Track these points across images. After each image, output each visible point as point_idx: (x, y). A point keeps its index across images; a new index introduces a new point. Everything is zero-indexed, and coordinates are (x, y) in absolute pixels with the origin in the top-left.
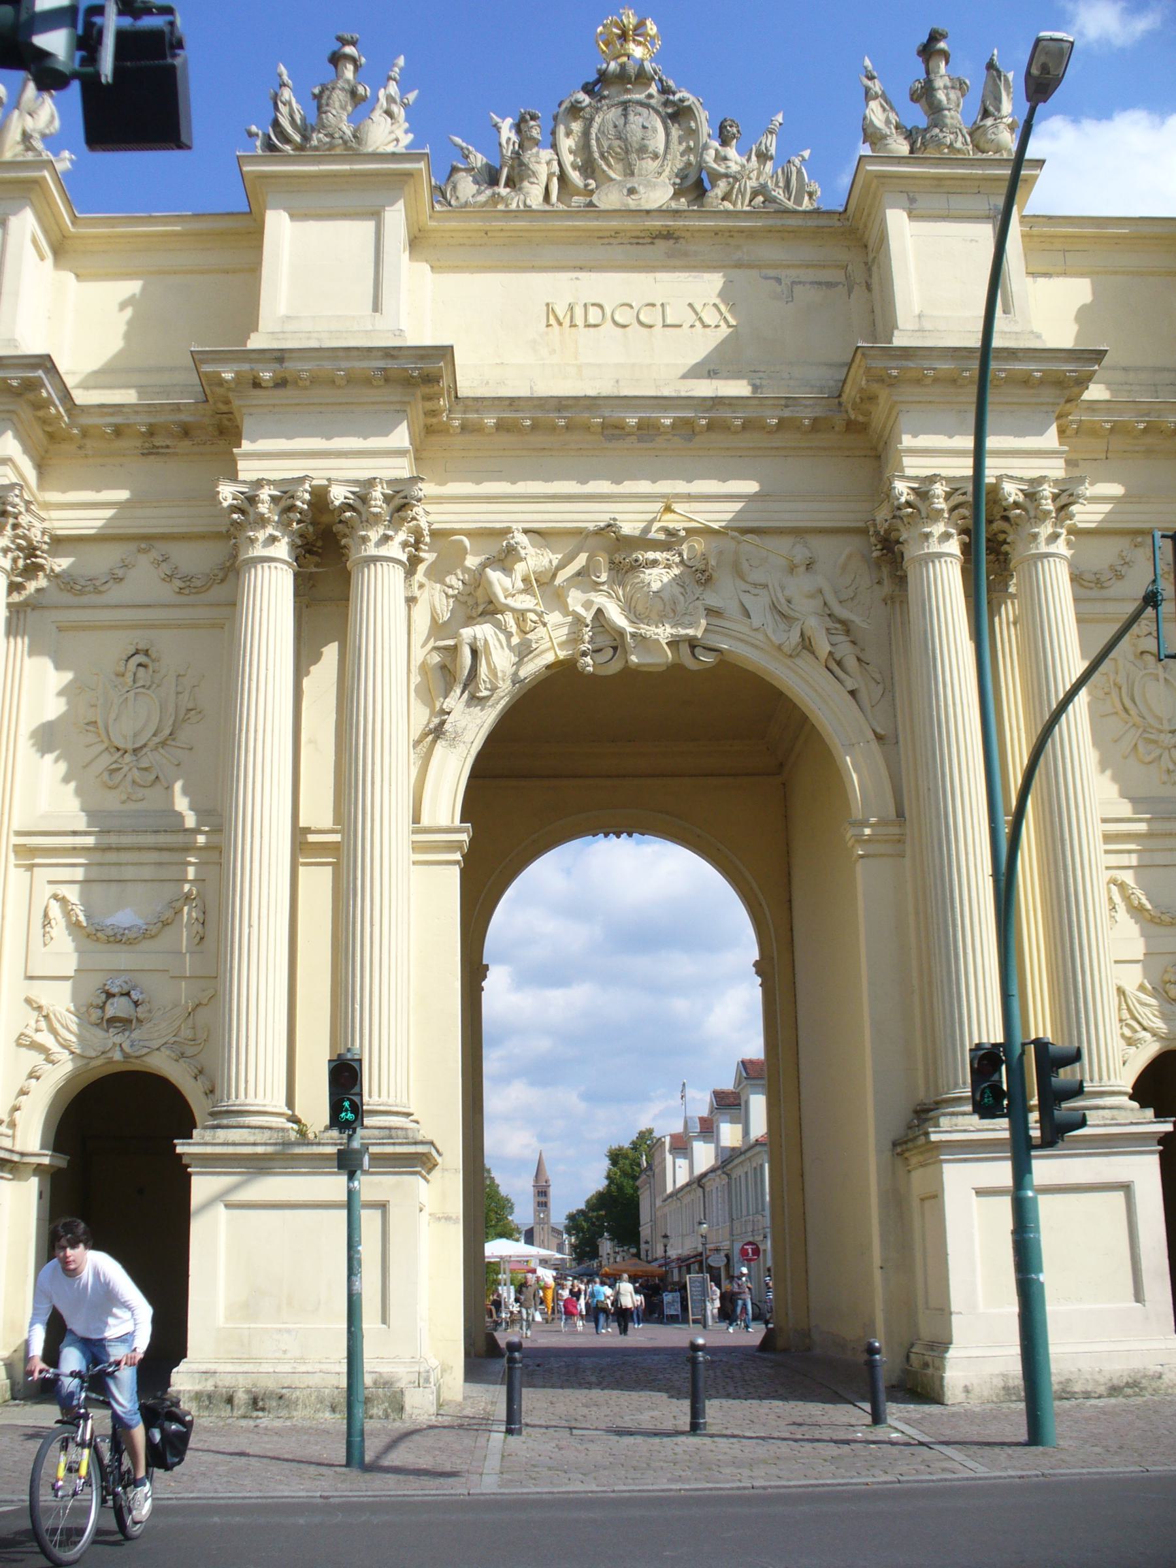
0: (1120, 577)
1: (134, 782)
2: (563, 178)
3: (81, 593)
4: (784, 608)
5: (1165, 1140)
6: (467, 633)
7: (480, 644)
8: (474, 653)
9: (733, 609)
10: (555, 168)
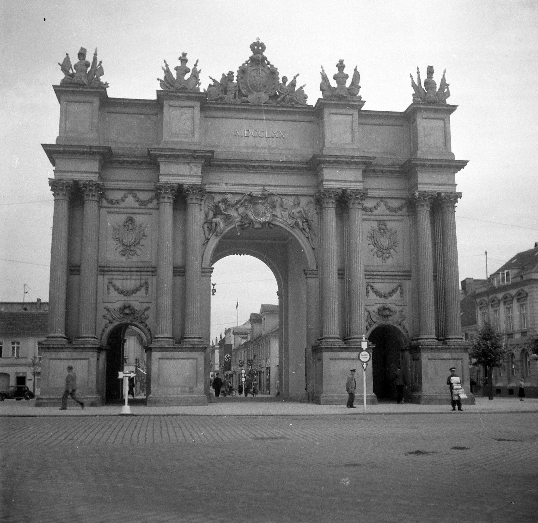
0: (376, 209)
1: (130, 254)
2: (239, 91)
3: (114, 204)
4: (291, 214)
5: (373, 349)
6: (214, 220)
7: (218, 223)
8: (216, 224)
9: (279, 215)
10: (238, 89)
